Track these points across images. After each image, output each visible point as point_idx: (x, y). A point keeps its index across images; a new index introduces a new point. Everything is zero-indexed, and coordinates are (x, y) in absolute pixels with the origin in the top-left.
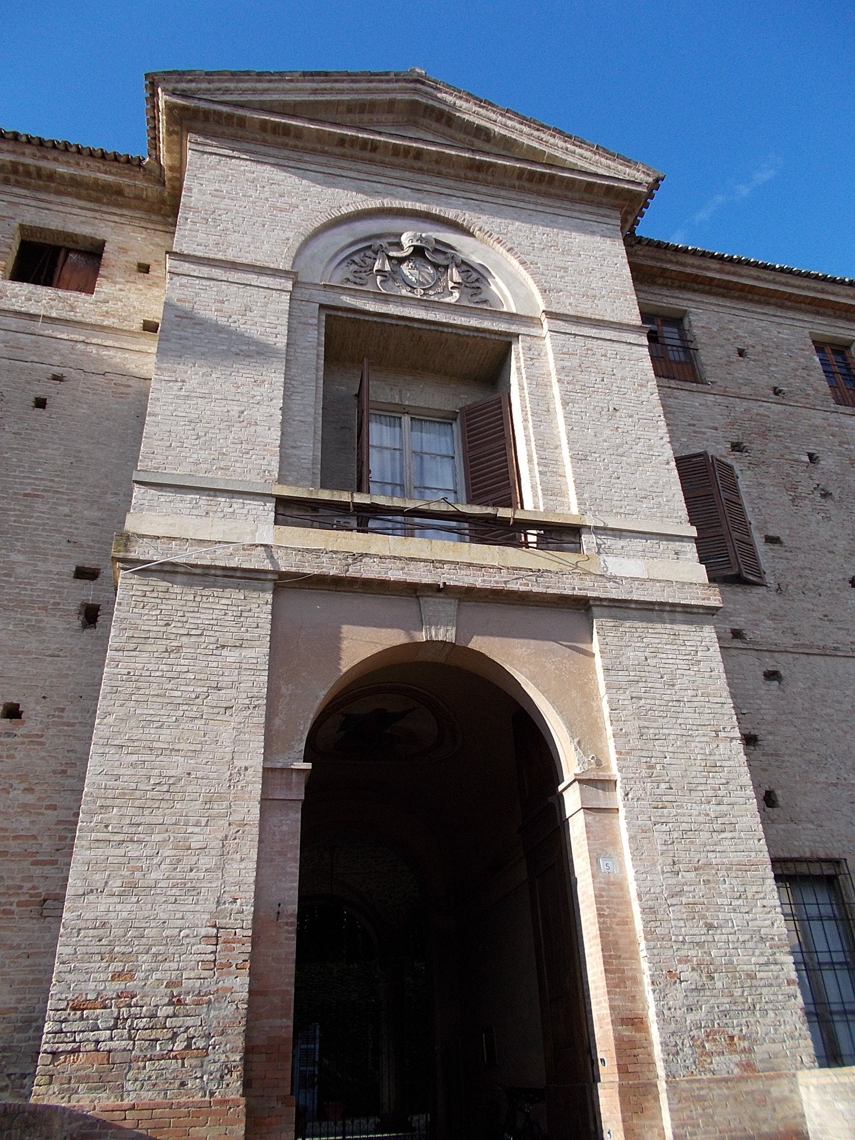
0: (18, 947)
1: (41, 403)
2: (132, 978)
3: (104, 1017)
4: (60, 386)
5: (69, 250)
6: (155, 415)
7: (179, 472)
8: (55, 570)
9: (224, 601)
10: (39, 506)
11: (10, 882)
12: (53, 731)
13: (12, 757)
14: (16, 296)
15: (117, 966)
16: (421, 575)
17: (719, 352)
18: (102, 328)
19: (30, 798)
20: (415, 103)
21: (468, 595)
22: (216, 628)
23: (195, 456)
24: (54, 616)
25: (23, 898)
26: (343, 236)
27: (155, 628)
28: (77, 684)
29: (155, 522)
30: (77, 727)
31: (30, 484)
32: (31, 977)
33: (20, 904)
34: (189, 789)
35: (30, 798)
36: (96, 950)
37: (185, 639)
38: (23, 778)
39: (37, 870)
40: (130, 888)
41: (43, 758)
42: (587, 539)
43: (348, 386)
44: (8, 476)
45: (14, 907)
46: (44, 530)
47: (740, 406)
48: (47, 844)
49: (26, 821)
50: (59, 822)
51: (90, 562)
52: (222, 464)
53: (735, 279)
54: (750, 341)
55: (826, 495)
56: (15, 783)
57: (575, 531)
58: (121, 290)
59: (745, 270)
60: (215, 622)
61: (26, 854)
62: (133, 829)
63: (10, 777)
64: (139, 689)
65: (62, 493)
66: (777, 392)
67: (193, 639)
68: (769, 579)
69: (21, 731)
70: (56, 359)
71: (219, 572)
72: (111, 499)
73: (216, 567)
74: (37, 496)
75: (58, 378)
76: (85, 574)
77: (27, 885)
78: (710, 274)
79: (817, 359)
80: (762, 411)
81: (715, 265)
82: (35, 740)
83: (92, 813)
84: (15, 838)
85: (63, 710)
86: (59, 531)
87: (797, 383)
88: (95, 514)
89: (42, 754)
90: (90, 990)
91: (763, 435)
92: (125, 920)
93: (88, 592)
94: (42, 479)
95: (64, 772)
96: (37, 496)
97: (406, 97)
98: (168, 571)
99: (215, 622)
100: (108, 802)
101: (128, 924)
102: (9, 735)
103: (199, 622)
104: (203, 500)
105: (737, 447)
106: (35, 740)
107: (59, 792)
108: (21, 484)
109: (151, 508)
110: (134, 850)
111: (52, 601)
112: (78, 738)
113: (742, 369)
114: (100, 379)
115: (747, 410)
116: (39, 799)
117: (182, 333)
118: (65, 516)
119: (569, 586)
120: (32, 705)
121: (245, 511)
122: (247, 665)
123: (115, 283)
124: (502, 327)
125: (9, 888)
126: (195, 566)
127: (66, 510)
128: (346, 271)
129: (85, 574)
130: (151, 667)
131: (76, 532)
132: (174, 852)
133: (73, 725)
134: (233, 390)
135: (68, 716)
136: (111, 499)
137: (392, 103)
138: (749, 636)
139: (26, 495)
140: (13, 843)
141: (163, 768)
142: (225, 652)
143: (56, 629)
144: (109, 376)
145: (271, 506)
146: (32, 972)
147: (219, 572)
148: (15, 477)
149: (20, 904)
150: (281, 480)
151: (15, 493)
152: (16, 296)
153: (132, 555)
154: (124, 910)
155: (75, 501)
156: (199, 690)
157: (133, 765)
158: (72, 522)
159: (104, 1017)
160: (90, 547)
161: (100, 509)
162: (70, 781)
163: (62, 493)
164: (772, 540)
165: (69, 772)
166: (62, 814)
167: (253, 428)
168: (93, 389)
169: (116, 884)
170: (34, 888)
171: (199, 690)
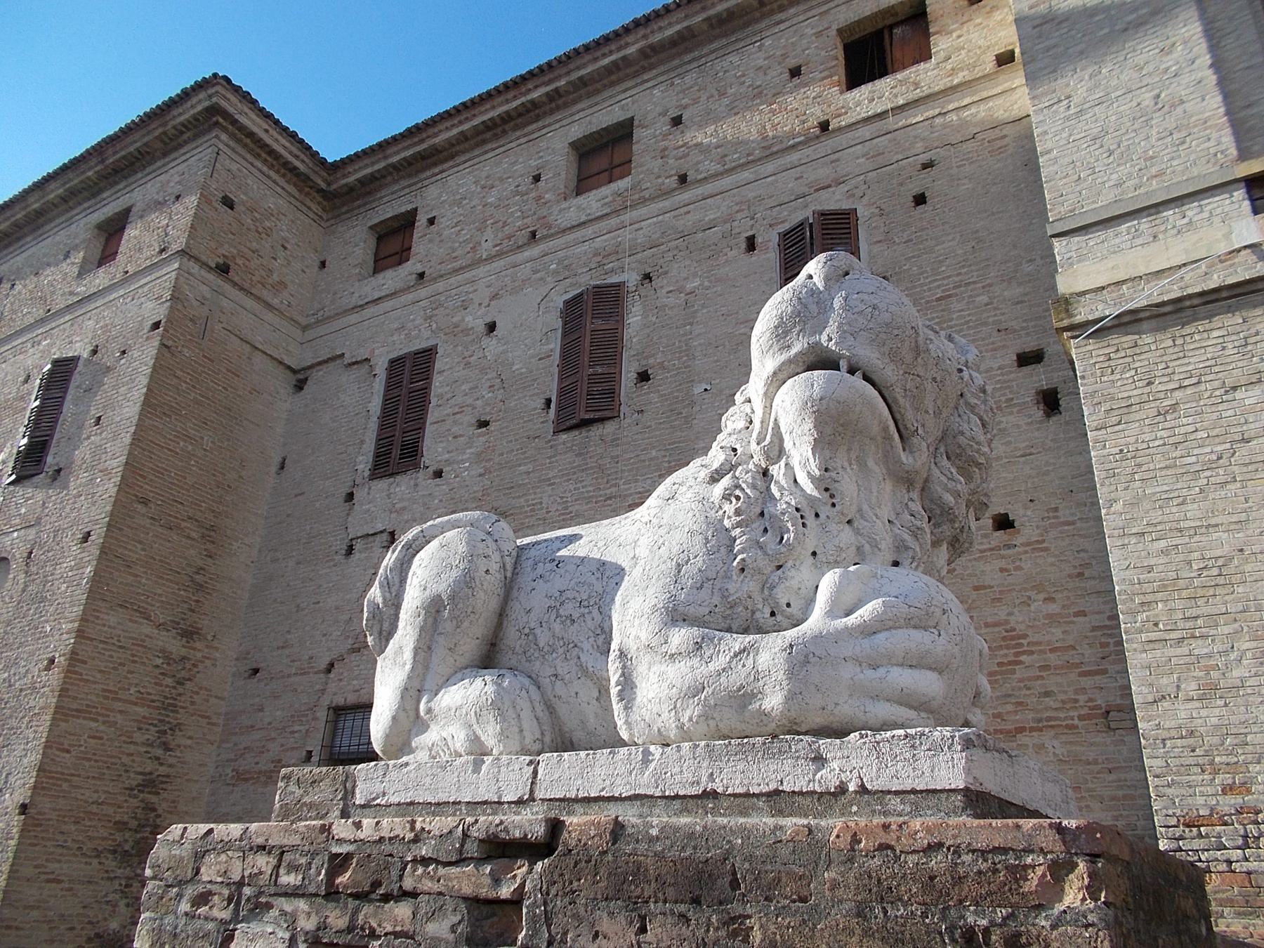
0: (1096, 762)
1: (920, 200)
2: (1249, 792)
3: (1230, 836)
4: (933, 172)
5: (891, 27)
6: (1049, 152)
7: (1102, 202)
8: (996, 366)
9: (1215, 334)
10: (956, 305)
11: (1064, 697)
12: (1053, 534)
13: (1018, 568)
14: (858, 104)
15: (1223, 778)
18: (953, 89)
19: (1053, 608)
22: (1216, 369)
23: (1115, 176)
24: (1011, 413)
25: (1084, 711)
27: (1135, 392)
28: (1063, 478)
29: (1091, 272)
30: (1079, 524)
31: (939, 287)
32: (1120, 793)
33: (1081, 718)
34: (1248, 568)
35: (1053, 608)
36: (1191, 761)
37: (1178, 394)
38: (1039, 588)
39: (1087, 682)
40: (1209, 692)
41: (1052, 565)
44: (915, 287)
45: (1076, 722)
46: (969, 328)
48: (1089, 653)
49: (1057, 632)
50: (1094, 629)
51: (1030, 345)
52: (1154, 171)
56: (1032, 594)
58: (959, 37)
60: (1213, 362)
61: (1070, 666)
62: (1190, 624)
63: (1026, 590)
64: (1140, 465)
65: (974, 283)
67: (1189, 391)
69: (1019, 540)
70: (919, 146)
71: (1196, 301)
72: (1028, 268)
73: (1190, 296)
74: (949, 296)
75: (927, 165)
76: (1028, 359)
77: (1082, 698)
82: (1037, 546)
83: (1133, 613)
84: (1052, 650)
85: (1056, 509)
86: (985, 324)
88: (1017, 291)
89: (1051, 560)
90: (1200, 804)
92: (1216, 726)
93: (1039, 377)
94: (949, 277)
95: (1081, 575)
96: (949, 296)
98: (1129, 321)
99: (1213, 362)
100: (1149, 598)
101: (1222, 730)
102: (1008, 547)
103: (1190, 368)
104: (1144, 224)
106: (1037, 546)
107: (1083, 596)
108: (930, 290)
109: (1081, 258)
110: (1200, 648)
111: (1003, 399)
112: (1084, 536)
114: (970, 146)
116: (1064, 606)
117: (1047, 43)
118: (987, 305)
120: (1021, 512)
121: (1206, 215)
123: (951, 33)
125: (1063, 702)
126: (1163, 304)
127: (984, 299)
129: (1028, 359)
130: (1147, 437)
131: (1003, 318)
132: (1254, 644)
133: (1073, 523)
134: (1135, 75)
135: (1064, 514)
136: (1028, 268)
139: (938, 299)
140: (1052, 656)
141: (1204, 549)
142: (1239, 394)
143: (1018, 426)
144: (979, 137)
145: (1240, 194)
146: (1121, 787)
147: (1196, 301)
148: (921, 285)
149: (1081, 718)
150: (1244, 155)
151: (928, 302)
152: (858, 104)
153: (1079, 319)
154: (1213, 715)
155: (990, 285)
156: (1219, 448)
157: (1164, 552)
158: (995, 309)
159: (1230, 836)
160: (1023, 328)
161: (1020, 284)
162: (1093, 582)
163: (974, 283)
165: (1087, 574)
166: (1096, 620)
167: (1179, 110)
168: (967, 159)
169: (1190, 687)
170: (1091, 700)
171: (1219, 448)
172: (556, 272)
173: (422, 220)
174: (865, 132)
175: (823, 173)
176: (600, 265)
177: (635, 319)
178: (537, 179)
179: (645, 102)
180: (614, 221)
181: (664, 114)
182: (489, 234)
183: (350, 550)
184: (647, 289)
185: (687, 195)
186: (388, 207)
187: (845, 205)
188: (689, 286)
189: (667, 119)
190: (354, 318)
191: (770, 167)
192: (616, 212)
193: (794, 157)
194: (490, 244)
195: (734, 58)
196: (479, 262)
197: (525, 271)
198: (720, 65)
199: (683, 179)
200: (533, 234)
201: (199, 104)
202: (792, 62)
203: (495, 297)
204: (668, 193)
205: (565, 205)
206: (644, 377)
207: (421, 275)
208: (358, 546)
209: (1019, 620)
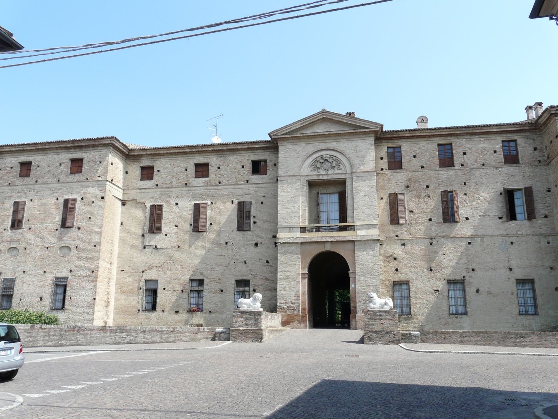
10: (265, 225)
16: (324, 240)
17: (408, 158)
20: (324, 118)
21: (332, 242)
26: (310, 160)
29: (282, 236)
42: (355, 227)
43: (315, 192)
47: (410, 174)
53: (414, 135)
54: (418, 152)
55: (429, 196)
57: (354, 226)
59: (417, 132)
66: (422, 167)
68: (408, 222)
70: (263, 192)
78: (406, 135)
79: (437, 153)
80: (416, 175)
81: (407, 132)
82: (271, 266)
87: (429, 163)
90: (282, 302)
91: (415, 182)
97: (322, 117)
105: (407, 187)
106: (271, 266)
113: (414, 161)
115: (412, 175)
119: (351, 239)
122: (297, 258)
124: (343, 176)
128: (311, 169)
137: (319, 120)
138: (400, 236)
154: (285, 292)
164: (411, 212)
172: (192, 195)
173: (156, 170)
174: (255, 186)
175: (247, 191)
176: (202, 197)
177: (209, 211)
178: (186, 170)
179: (213, 161)
180: (205, 188)
181: (216, 165)
182: (175, 180)
183: (145, 248)
184: (212, 206)
185: (220, 187)
186: (146, 163)
187: (250, 200)
188: (221, 208)
189: (217, 167)
190: (139, 191)
191: (237, 187)
192: (205, 186)
193: (242, 186)
194: (175, 183)
195: (231, 157)
196: (172, 187)
197: (184, 193)
198: (229, 158)
199: (220, 183)
200: (186, 184)
201: (107, 142)
202: (243, 164)
203: (177, 197)
204: (216, 185)
205: (194, 179)
206: (211, 224)
207: (157, 185)
208: (147, 247)
209: (268, 276)
